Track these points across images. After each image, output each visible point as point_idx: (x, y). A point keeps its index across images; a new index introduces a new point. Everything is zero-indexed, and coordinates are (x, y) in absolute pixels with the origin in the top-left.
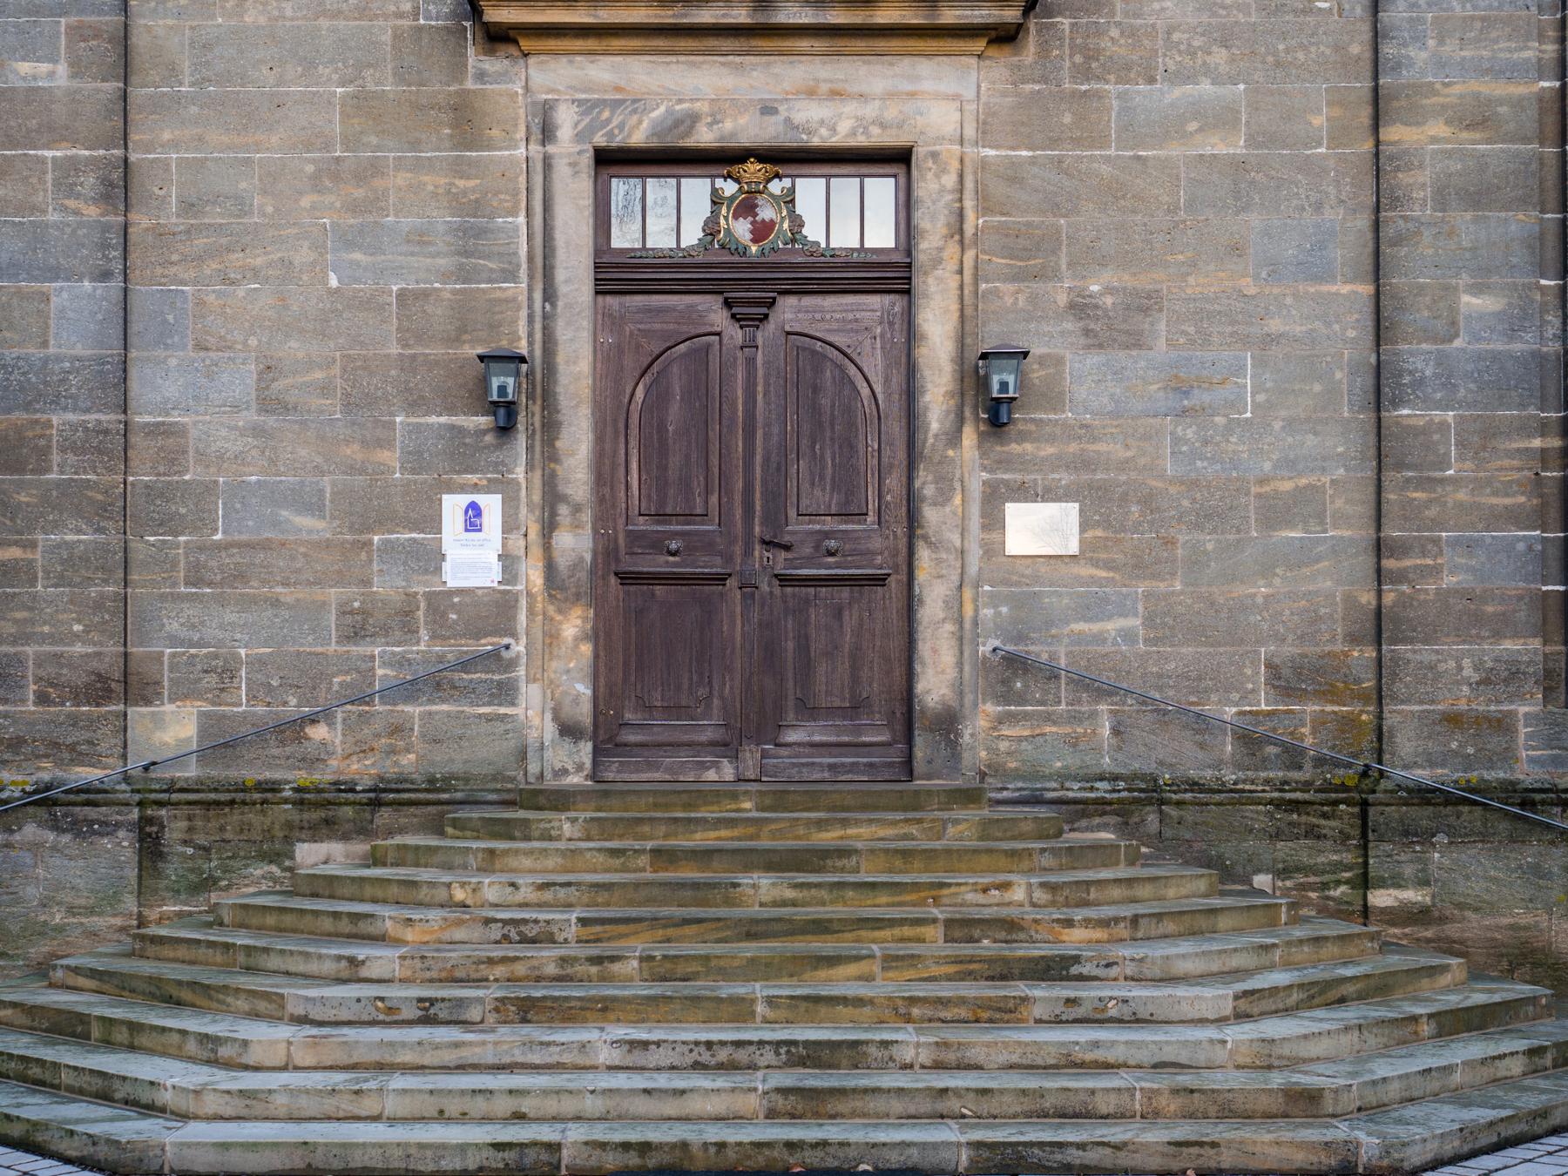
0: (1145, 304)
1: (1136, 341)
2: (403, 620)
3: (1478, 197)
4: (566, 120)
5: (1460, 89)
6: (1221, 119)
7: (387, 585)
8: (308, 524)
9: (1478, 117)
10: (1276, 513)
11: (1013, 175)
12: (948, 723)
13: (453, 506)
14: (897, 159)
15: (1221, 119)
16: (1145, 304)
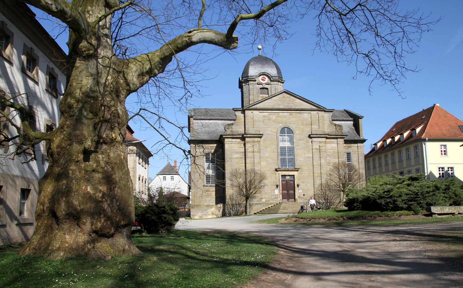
0: (304, 181)
1: (304, 183)
2: (274, 195)
3: (318, 177)
4: (280, 174)
5: (317, 172)
6: (307, 173)
7: (273, 194)
8: (270, 191)
9: (317, 173)
10: (310, 190)
11: (298, 176)
12: (297, 199)
13: (276, 190)
14: (294, 176)
15: (307, 173)
16: (304, 181)
